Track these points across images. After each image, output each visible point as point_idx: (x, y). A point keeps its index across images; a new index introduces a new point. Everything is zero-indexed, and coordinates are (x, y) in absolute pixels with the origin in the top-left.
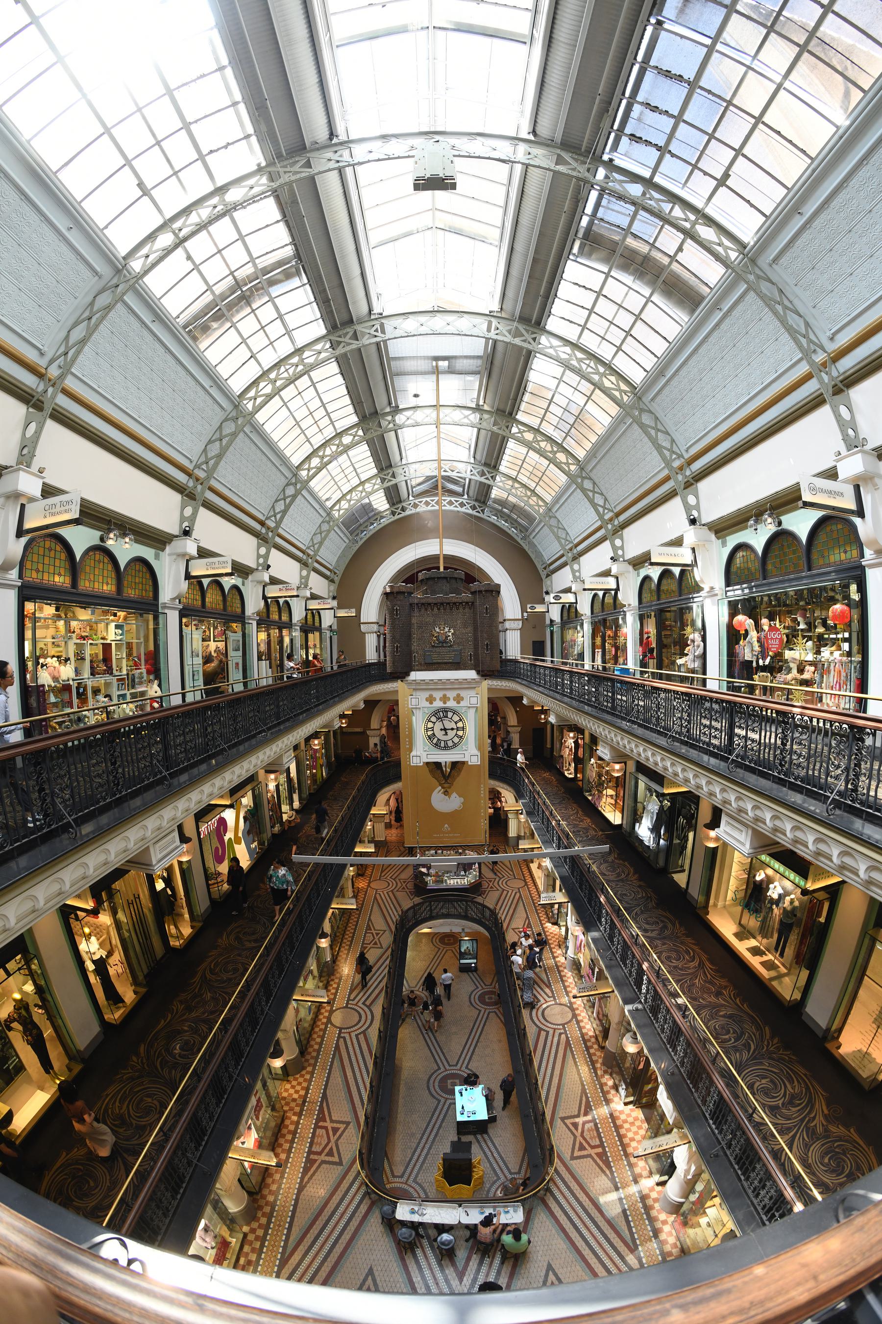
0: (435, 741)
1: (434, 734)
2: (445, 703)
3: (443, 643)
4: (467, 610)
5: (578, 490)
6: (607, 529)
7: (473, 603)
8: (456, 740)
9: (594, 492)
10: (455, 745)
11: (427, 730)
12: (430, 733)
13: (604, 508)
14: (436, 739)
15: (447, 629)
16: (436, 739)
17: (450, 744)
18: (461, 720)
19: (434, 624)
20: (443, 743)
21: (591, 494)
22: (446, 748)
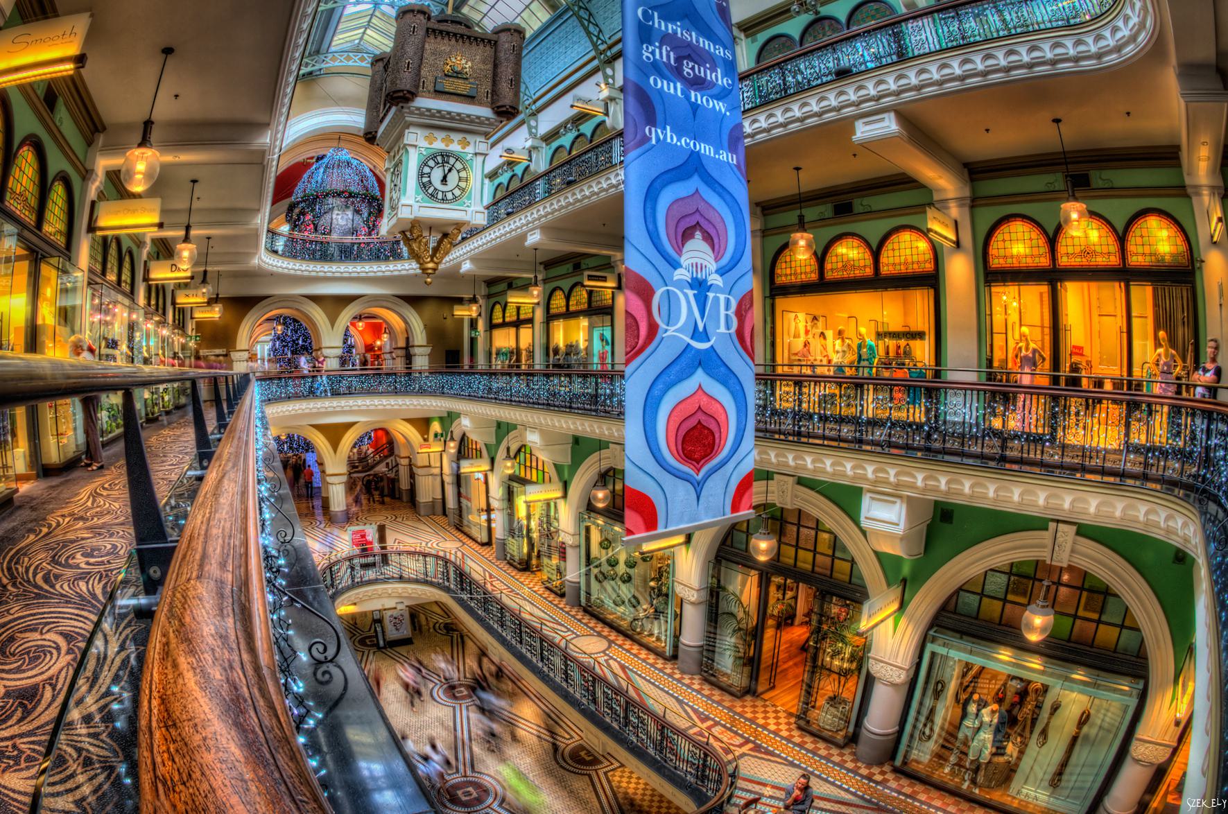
0: (430, 191)
1: (430, 182)
2: (447, 146)
3: (457, 75)
4: (488, 48)
5: (574, 18)
6: (599, 59)
7: (496, 42)
8: (457, 192)
9: (589, 21)
10: (455, 198)
11: (421, 175)
12: (425, 180)
13: (598, 38)
14: (432, 189)
15: (464, 61)
16: (432, 189)
17: (450, 196)
18: (464, 169)
19: (449, 54)
20: (440, 194)
21: (586, 23)
22: (444, 200)
